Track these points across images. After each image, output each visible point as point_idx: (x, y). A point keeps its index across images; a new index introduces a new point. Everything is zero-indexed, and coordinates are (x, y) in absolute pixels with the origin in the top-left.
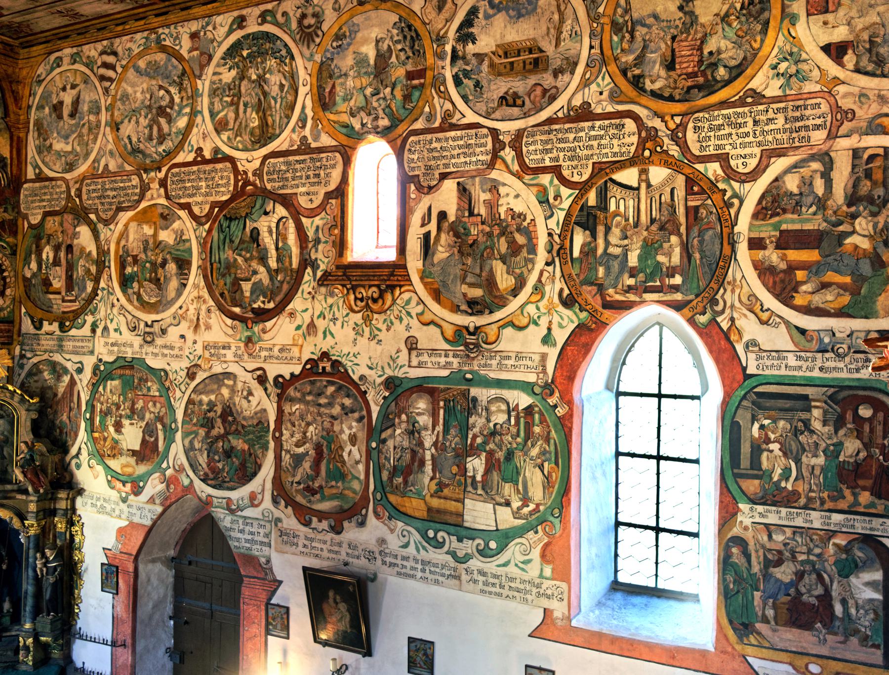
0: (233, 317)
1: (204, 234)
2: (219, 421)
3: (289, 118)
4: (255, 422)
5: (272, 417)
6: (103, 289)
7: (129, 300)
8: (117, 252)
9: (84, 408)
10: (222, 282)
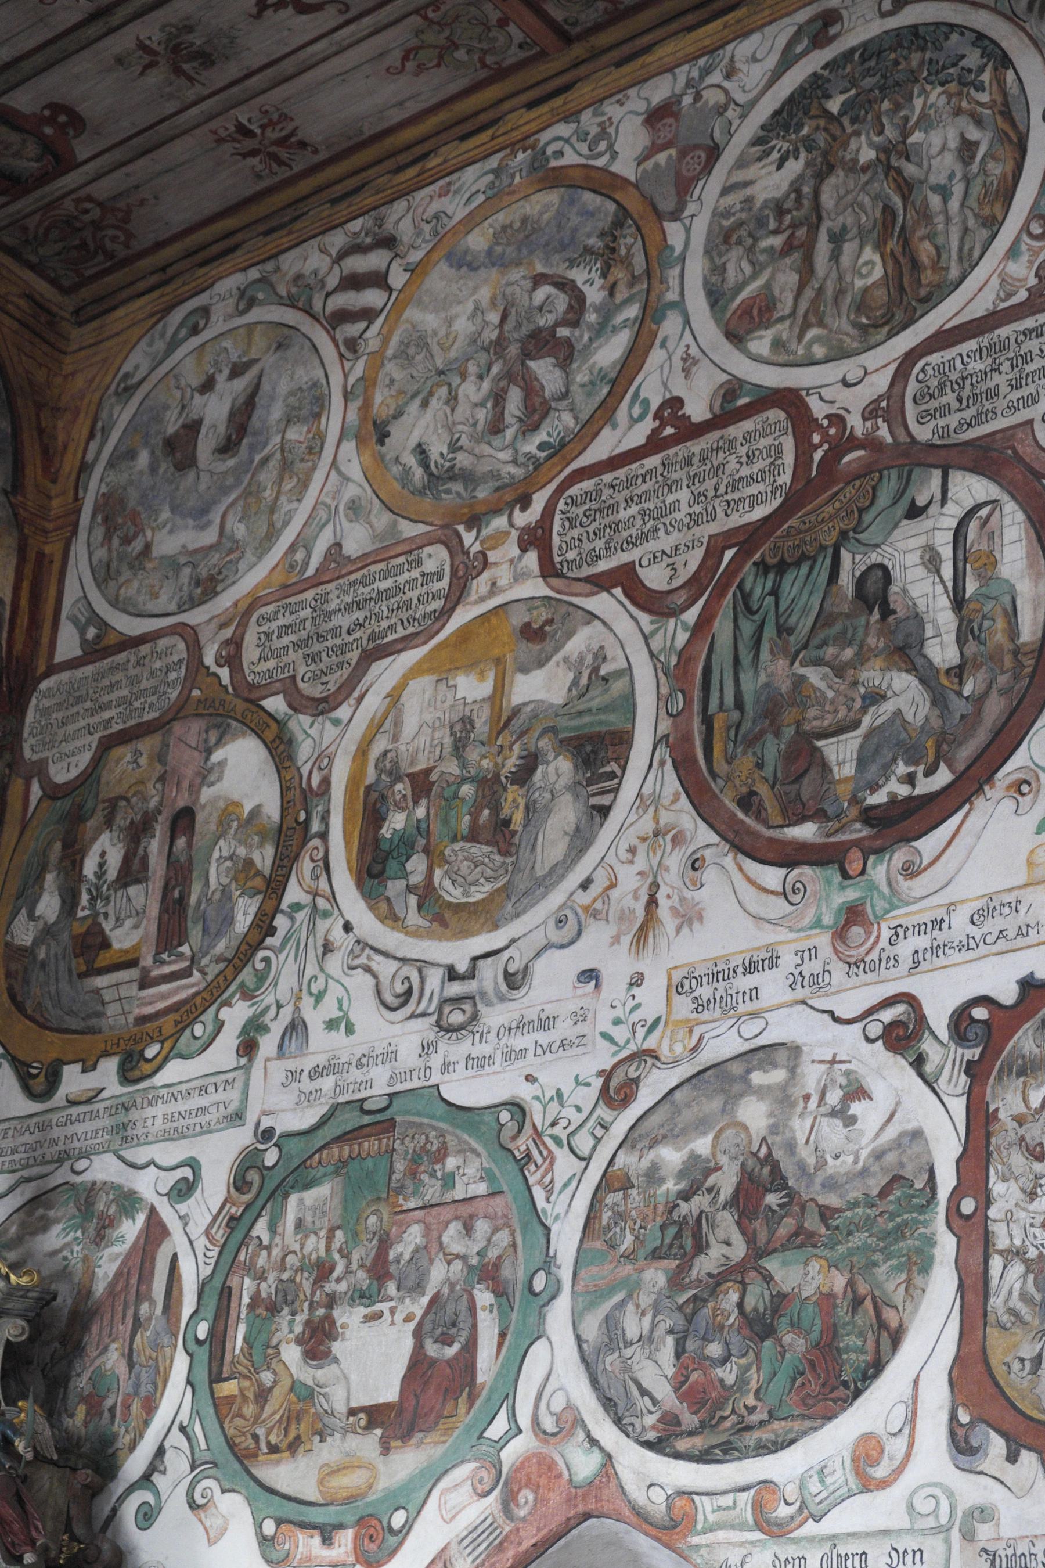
0: (789, 857)
1: (682, 638)
2: (727, 1221)
3: (993, 224)
4: (874, 1186)
5: (946, 1151)
6: (297, 907)
7: (391, 918)
8: (354, 781)
9: (188, 1307)
10: (746, 762)
